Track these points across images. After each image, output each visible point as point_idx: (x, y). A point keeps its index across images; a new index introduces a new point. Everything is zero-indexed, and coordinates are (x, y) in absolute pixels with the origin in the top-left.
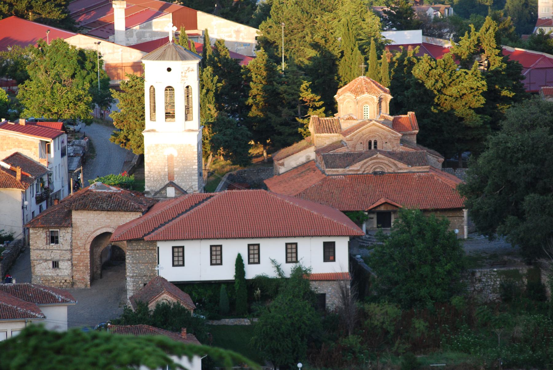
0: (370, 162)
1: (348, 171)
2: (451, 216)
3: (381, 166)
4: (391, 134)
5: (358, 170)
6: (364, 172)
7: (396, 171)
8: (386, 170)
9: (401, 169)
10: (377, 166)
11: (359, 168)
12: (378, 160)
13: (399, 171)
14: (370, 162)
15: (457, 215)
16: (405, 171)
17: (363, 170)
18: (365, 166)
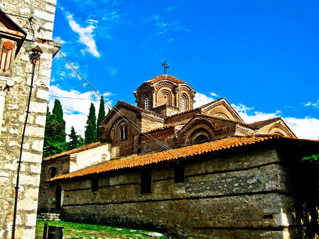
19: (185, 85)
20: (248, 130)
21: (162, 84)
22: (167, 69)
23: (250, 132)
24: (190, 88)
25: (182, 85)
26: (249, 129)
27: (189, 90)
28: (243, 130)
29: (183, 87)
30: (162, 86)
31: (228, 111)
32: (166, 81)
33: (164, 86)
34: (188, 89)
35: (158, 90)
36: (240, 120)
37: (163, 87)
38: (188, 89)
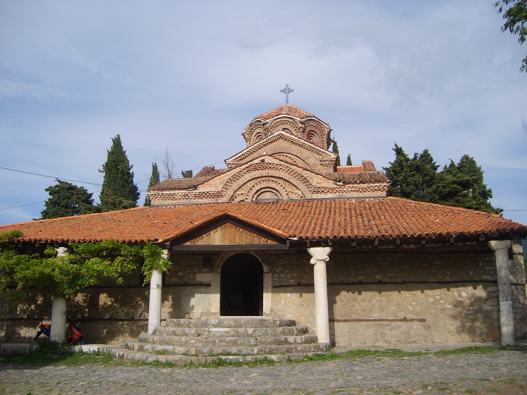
0: (248, 177)
1: (195, 196)
2: (448, 279)
3: (273, 185)
4: (315, 155)
5: (219, 195)
6: (232, 198)
7: (309, 196)
8: (284, 193)
9: (318, 190)
10: (265, 184)
11: (220, 188)
12: (264, 172)
13: (315, 196)
14: (248, 177)
15: (467, 278)
16: (329, 196)
17: (230, 193)
18: (235, 186)
19: (282, 117)
20: (175, 192)
21: (254, 127)
22: (291, 95)
23: (180, 194)
24: (292, 119)
25: (276, 119)
26: (176, 192)
27: (292, 121)
28: (169, 196)
29: (280, 120)
30: (255, 129)
31: (294, 145)
32: (256, 121)
33: (257, 128)
34: (289, 120)
35: (252, 136)
36: (323, 152)
37: (255, 129)
38: (289, 120)
